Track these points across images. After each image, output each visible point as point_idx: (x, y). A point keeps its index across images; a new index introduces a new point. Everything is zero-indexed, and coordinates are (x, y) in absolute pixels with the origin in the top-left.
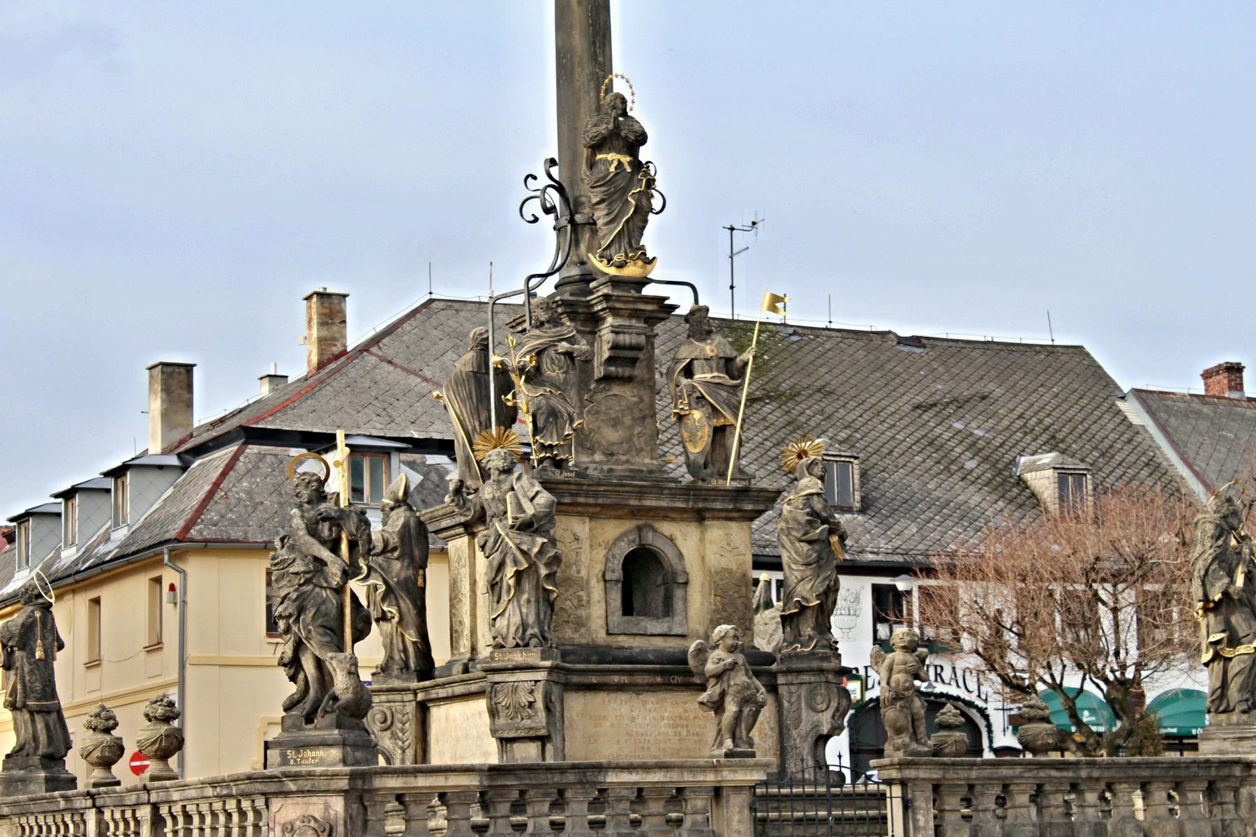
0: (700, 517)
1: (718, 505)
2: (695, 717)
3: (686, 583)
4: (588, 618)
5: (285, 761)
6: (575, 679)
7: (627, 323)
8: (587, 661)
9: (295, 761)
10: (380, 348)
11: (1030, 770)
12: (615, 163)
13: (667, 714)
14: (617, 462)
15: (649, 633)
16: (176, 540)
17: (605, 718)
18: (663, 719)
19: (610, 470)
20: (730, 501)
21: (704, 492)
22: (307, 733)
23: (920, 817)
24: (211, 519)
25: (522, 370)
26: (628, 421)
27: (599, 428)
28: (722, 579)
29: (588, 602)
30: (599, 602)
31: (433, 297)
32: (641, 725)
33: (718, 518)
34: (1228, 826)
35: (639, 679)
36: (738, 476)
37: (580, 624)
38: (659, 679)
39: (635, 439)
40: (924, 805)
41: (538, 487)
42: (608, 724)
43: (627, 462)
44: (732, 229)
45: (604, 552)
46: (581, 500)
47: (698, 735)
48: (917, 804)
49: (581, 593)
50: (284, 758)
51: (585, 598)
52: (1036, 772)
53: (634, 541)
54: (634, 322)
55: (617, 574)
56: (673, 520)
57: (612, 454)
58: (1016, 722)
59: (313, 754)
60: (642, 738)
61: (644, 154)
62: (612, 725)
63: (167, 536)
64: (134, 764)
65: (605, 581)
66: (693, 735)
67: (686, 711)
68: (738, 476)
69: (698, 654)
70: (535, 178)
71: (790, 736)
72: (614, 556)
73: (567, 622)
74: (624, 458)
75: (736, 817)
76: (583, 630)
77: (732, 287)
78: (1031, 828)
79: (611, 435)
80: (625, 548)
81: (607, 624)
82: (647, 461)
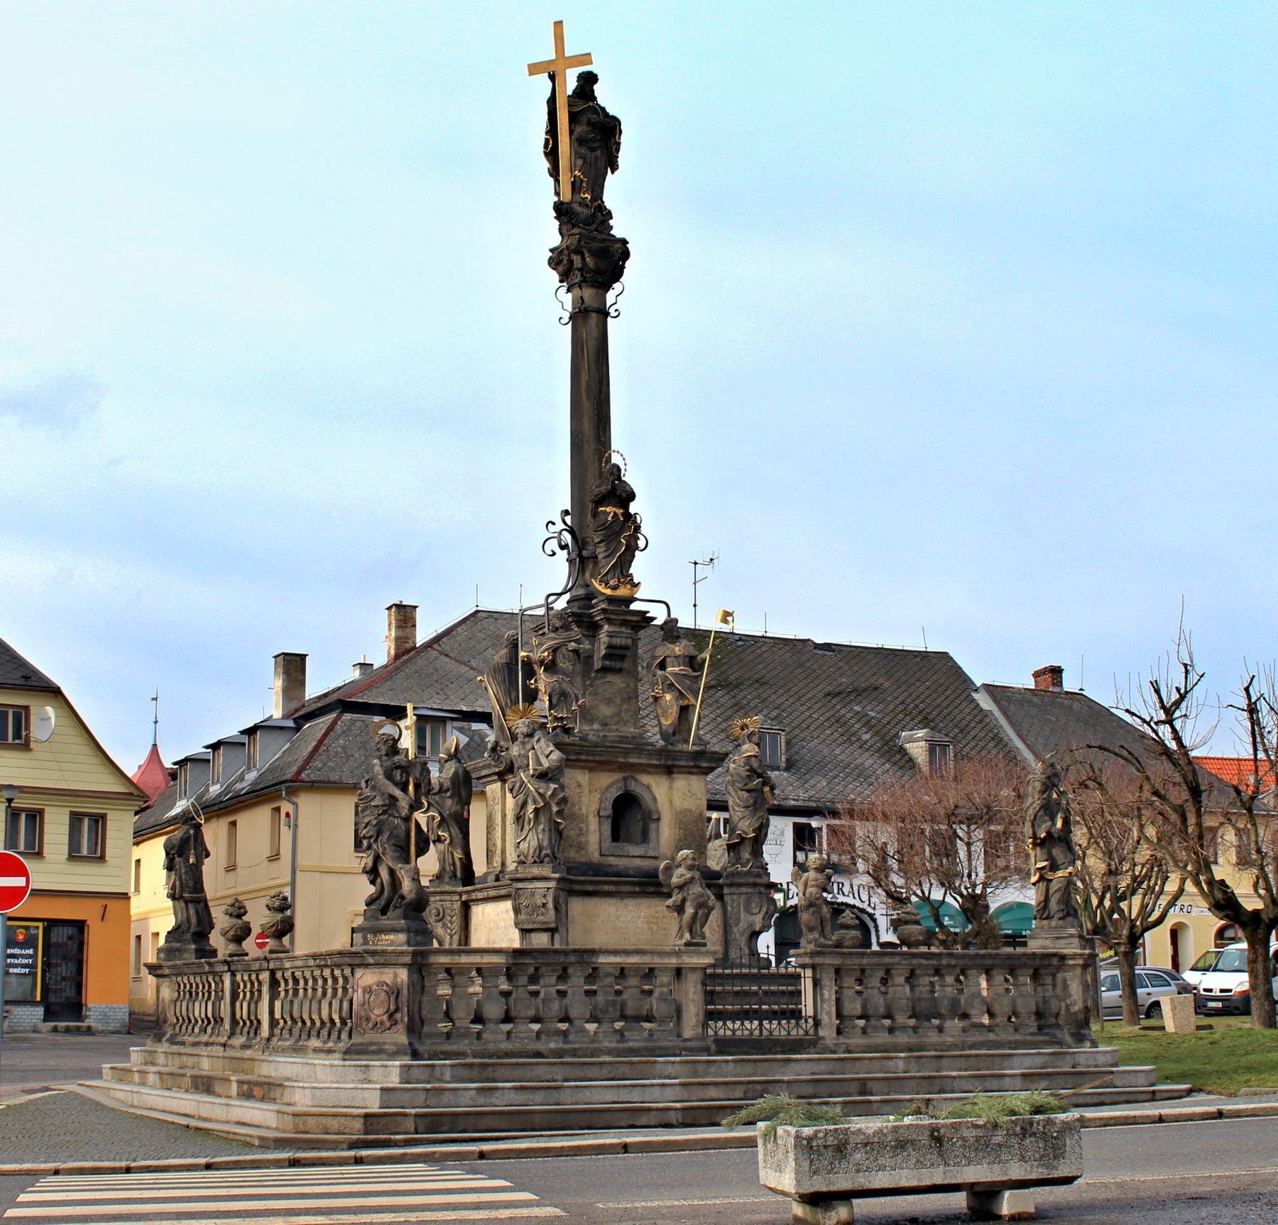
0: (669, 771)
1: (682, 763)
3: (659, 819)
4: (587, 843)
5: (366, 942)
6: (577, 887)
7: (618, 630)
8: (585, 874)
9: (373, 942)
10: (440, 645)
11: (905, 959)
12: (612, 514)
14: (610, 731)
16: (291, 781)
17: (598, 916)
18: (640, 918)
19: (605, 736)
20: (691, 760)
22: (382, 922)
23: (825, 992)
24: (317, 765)
25: (541, 663)
26: (618, 701)
27: (597, 705)
28: (684, 817)
29: (587, 831)
30: (594, 832)
31: (479, 609)
33: (682, 773)
34: (1048, 1001)
35: (623, 888)
36: (697, 742)
37: (581, 847)
39: (623, 714)
40: (828, 983)
41: (552, 748)
42: (600, 920)
43: (617, 730)
44: (696, 563)
45: (599, 796)
46: (583, 757)
48: (823, 982)
49: (581, 825)
50: (365, 938)
51: (585, 829)
53: (620, 788)
54: (623, 629)
55: (608, 811)
56: (650, 773)
57: (606, 725)
58: (896, 924)
59: (387, 937)
61: (633, 508)
62: (603, 921)
63: (285, 778)
64: (258, 941)
65: (599, 816)
67: (657, 912)
68: (697, 742)
69: (666, 871)
70: (554, 524)
71: (732, 932)
72: (606, 799)
73: (571, 846)
74: (614, 727)
75: (692, 990)
76: (583, 852)
77: (695, 606)
79: (606, 711)
80: (615, 793)
81: (600, 848)
82: (632, 730)
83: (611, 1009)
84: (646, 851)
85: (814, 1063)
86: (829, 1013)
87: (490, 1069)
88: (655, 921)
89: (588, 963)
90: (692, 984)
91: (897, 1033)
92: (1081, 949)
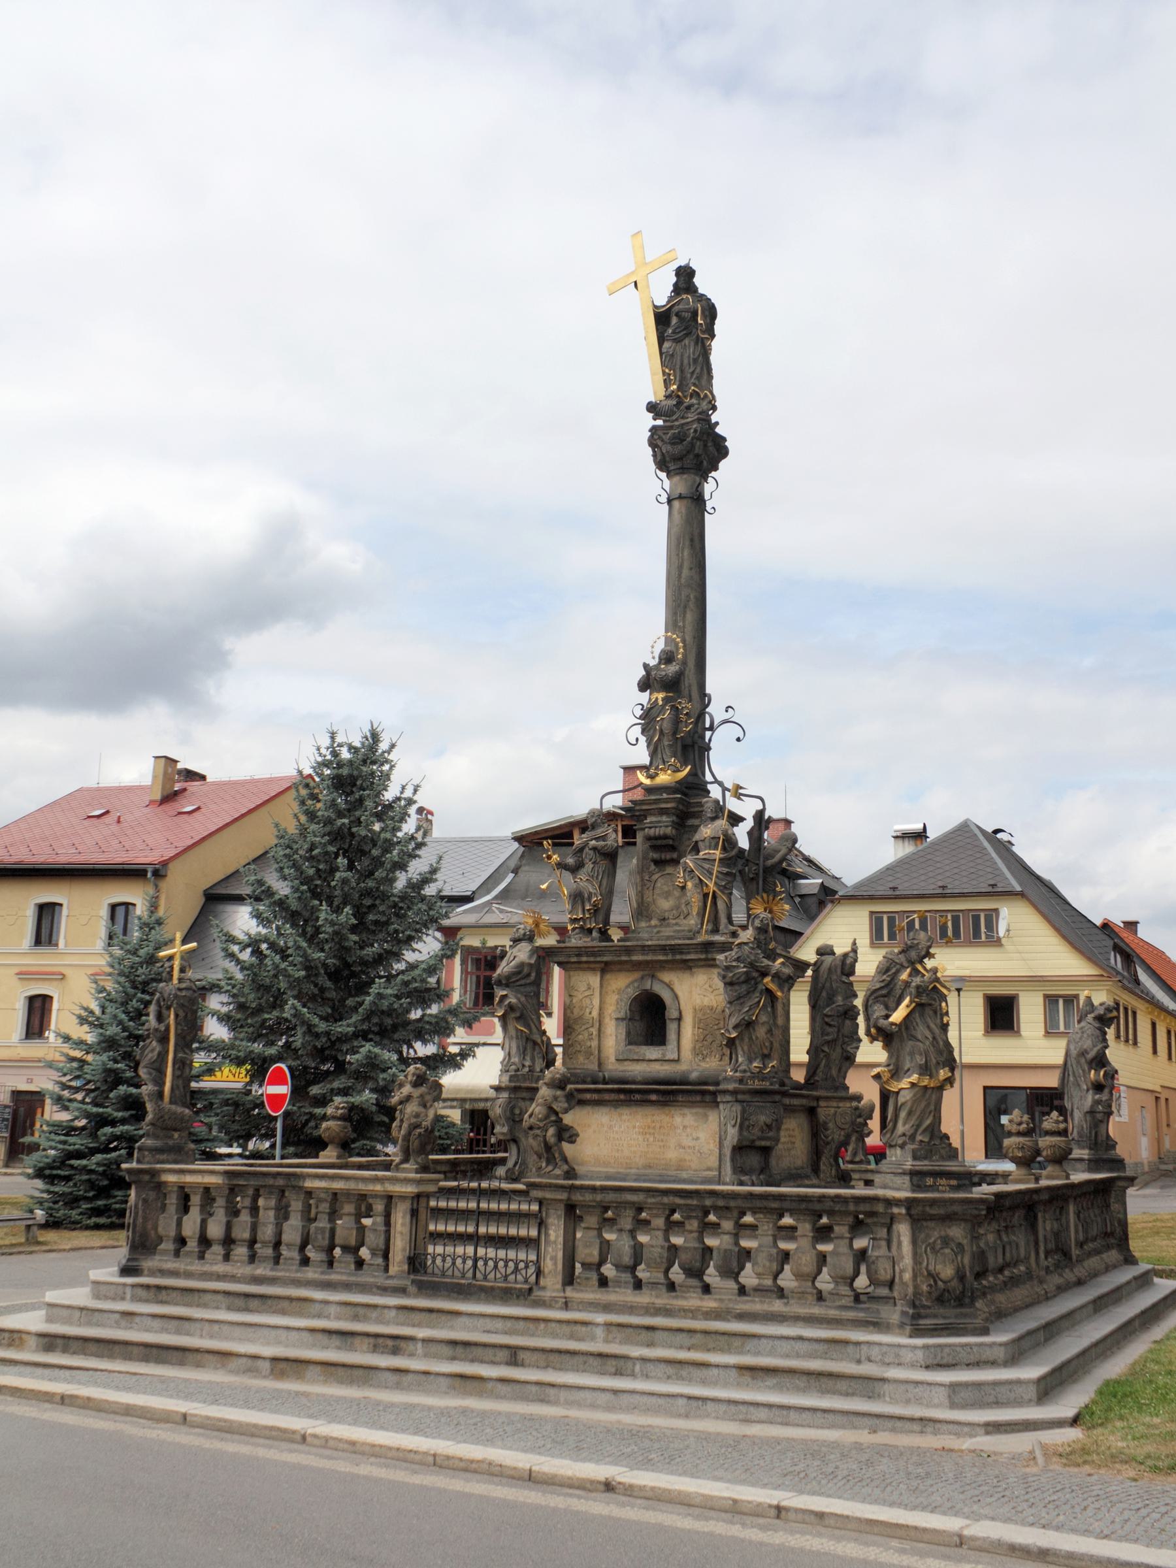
7: (659, 819)
11: (653, 1196)
15: (647, 1058)
17: (589, 1126)
18: (634, 1127)
20: (701, 952)
22: (79, 1142)
23: (551, 1232)
32: (617, 1133)
33: (702, 966)
34: (873, 1262)
35: (606, 1097)
39: (683, 906)
40: (556, 1222)
46: (584, 959)
47: (662, 1141)
49: (591, 1029)
52: (660, 1198)
56: (671, 969)
57: (664, 919)
62: (595, 1132)
73: (580, 1051)
74: (674, 922)
78: (659, 1250)
80: (632, 992)
83: (320, 1237)
84: (664, 1055)
85: (488, 1320)
86: (554, 1259)
87: (164, 1292)
88: (652, 1131)
89: (301, 1188)
90: (401, 1215)
91: (644, 1289)
92: (913, 1191)
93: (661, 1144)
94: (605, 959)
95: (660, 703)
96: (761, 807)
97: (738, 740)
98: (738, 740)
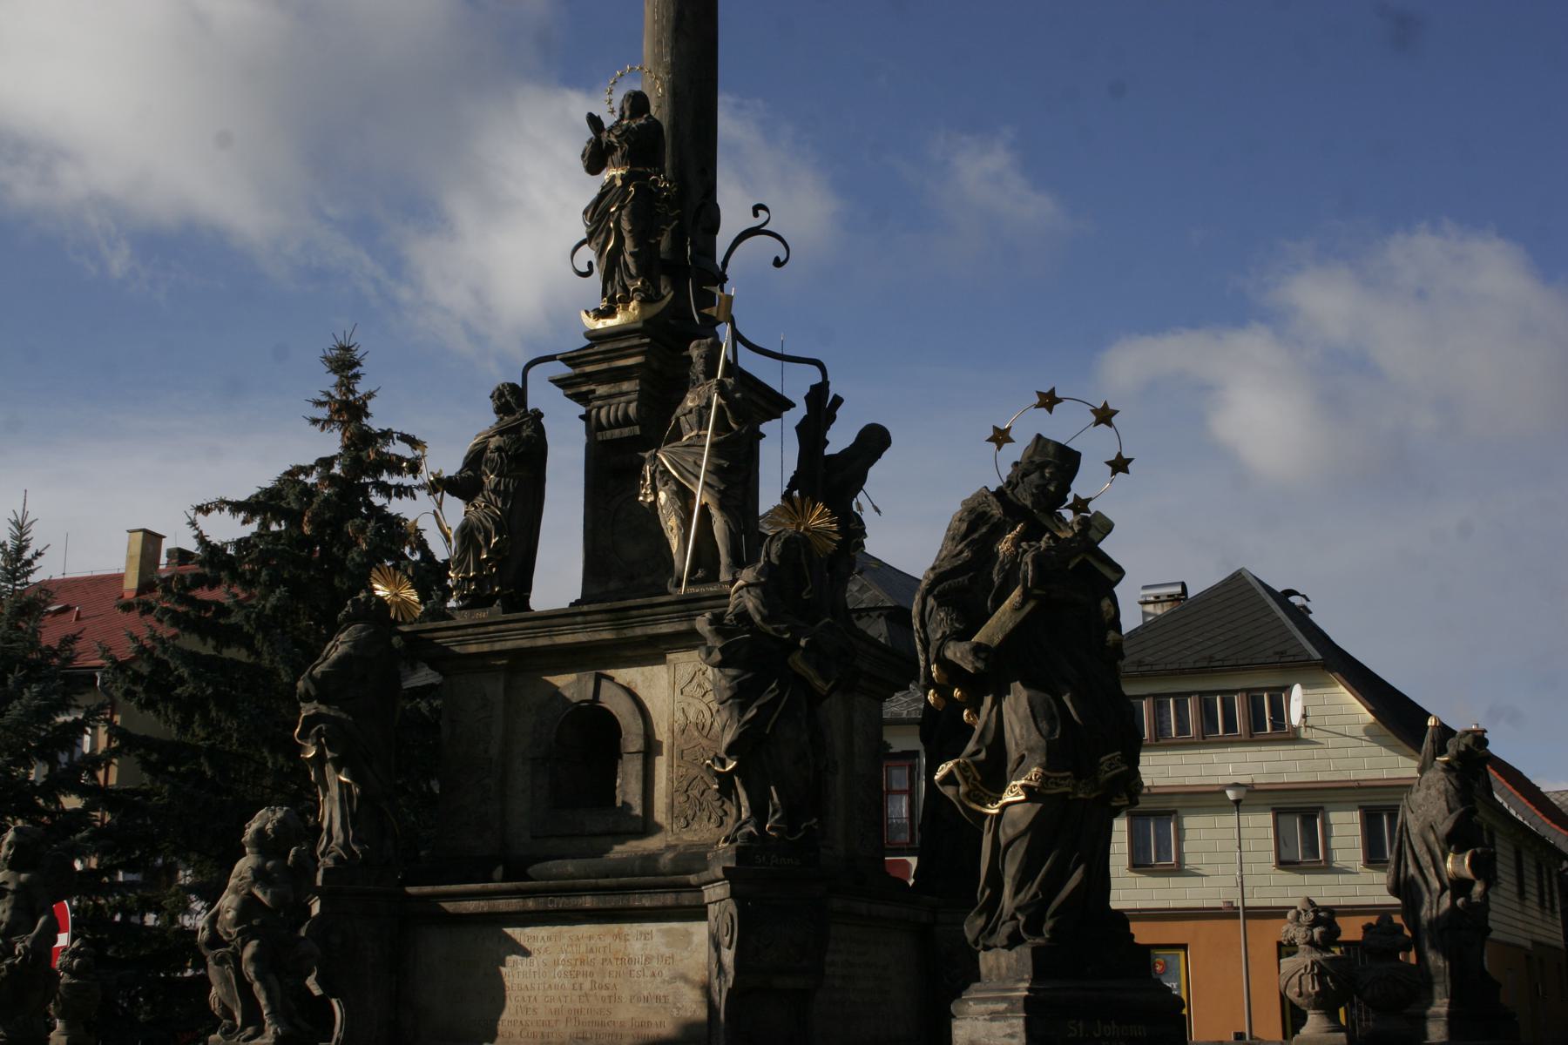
1: (665, 629)
2: (604, 960)
13: (563, 956)
18: (556, 963)
21: (635, 613)
38: (531, 904)
60: (526, 994)
66: (601, 988)
88: (587, 968)
93: (605, 993)
94: (509, 645)
95: (619, 183)
96: (818, 379)
97: (778, 263)
98: (778, 263)
